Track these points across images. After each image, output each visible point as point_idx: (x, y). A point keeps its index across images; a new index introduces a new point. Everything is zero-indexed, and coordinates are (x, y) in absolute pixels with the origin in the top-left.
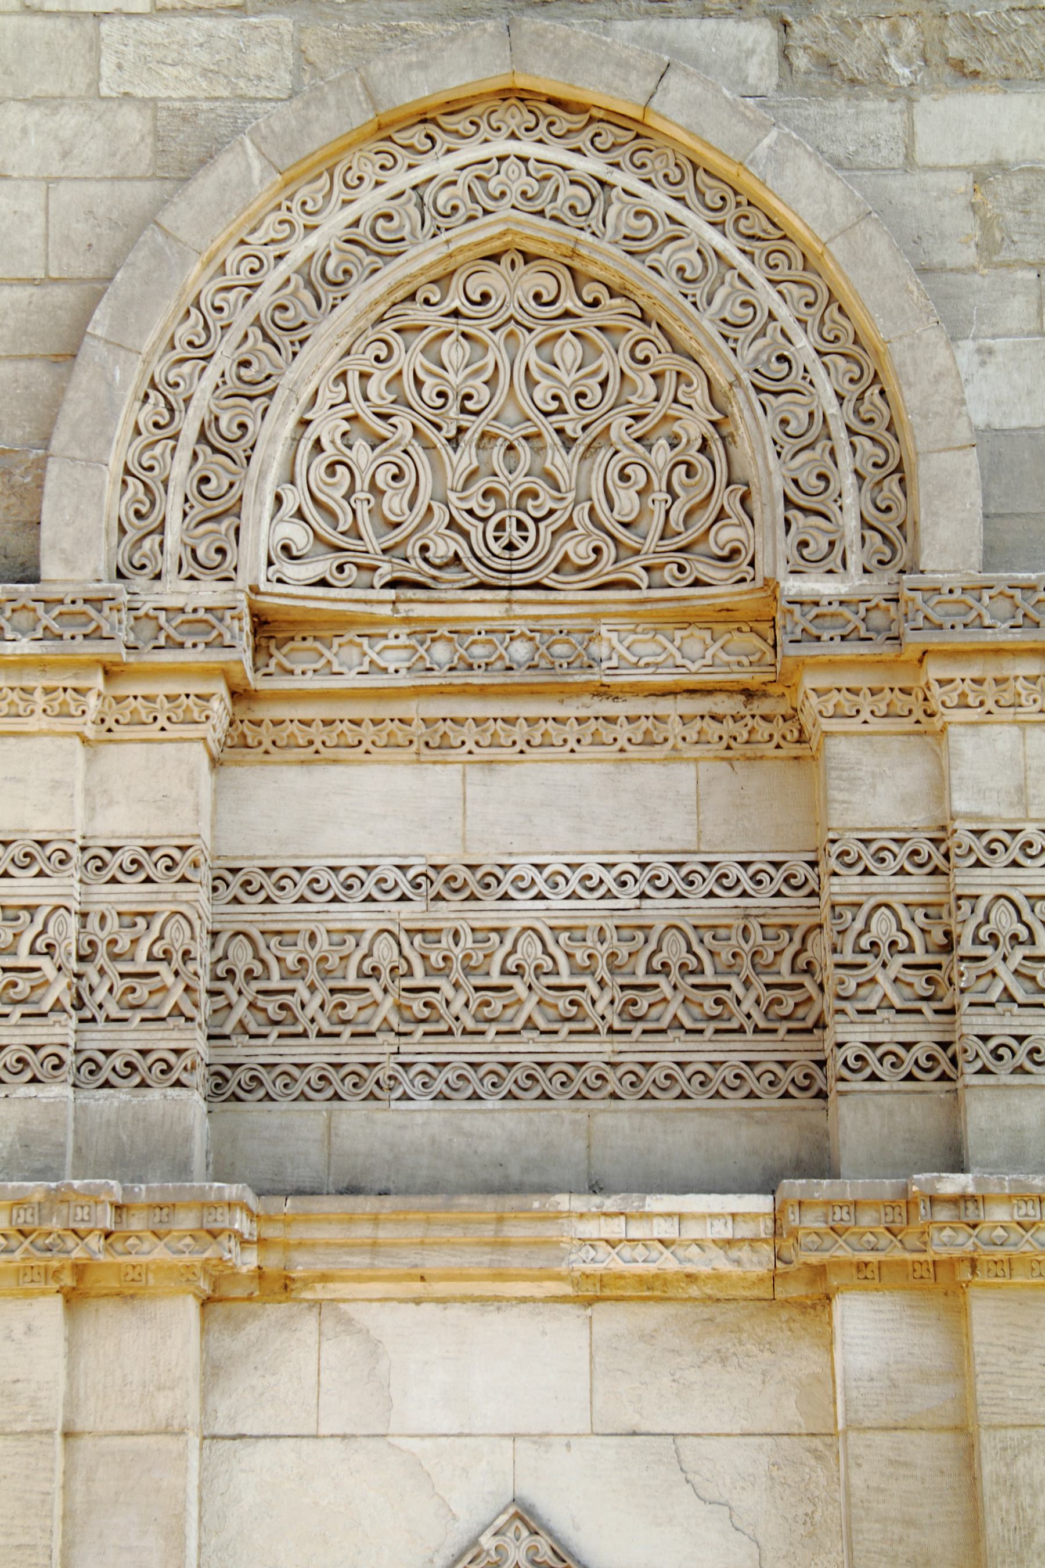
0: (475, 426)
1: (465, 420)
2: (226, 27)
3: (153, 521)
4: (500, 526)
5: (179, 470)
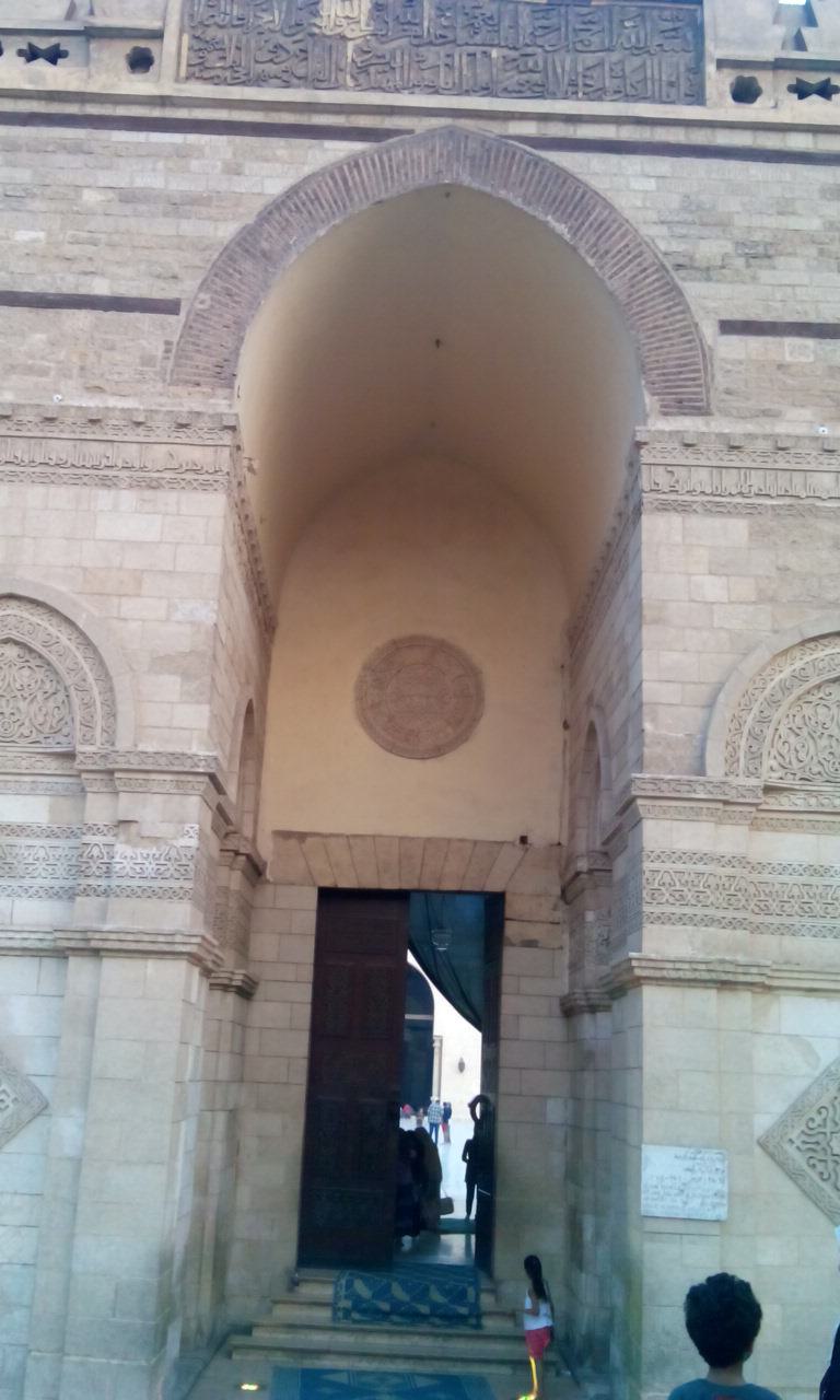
0: (827, 733)
1: (824, 731)
2: (751, 608)
3: (734, 759)
4: (834, 763)
5: (743, 743)
